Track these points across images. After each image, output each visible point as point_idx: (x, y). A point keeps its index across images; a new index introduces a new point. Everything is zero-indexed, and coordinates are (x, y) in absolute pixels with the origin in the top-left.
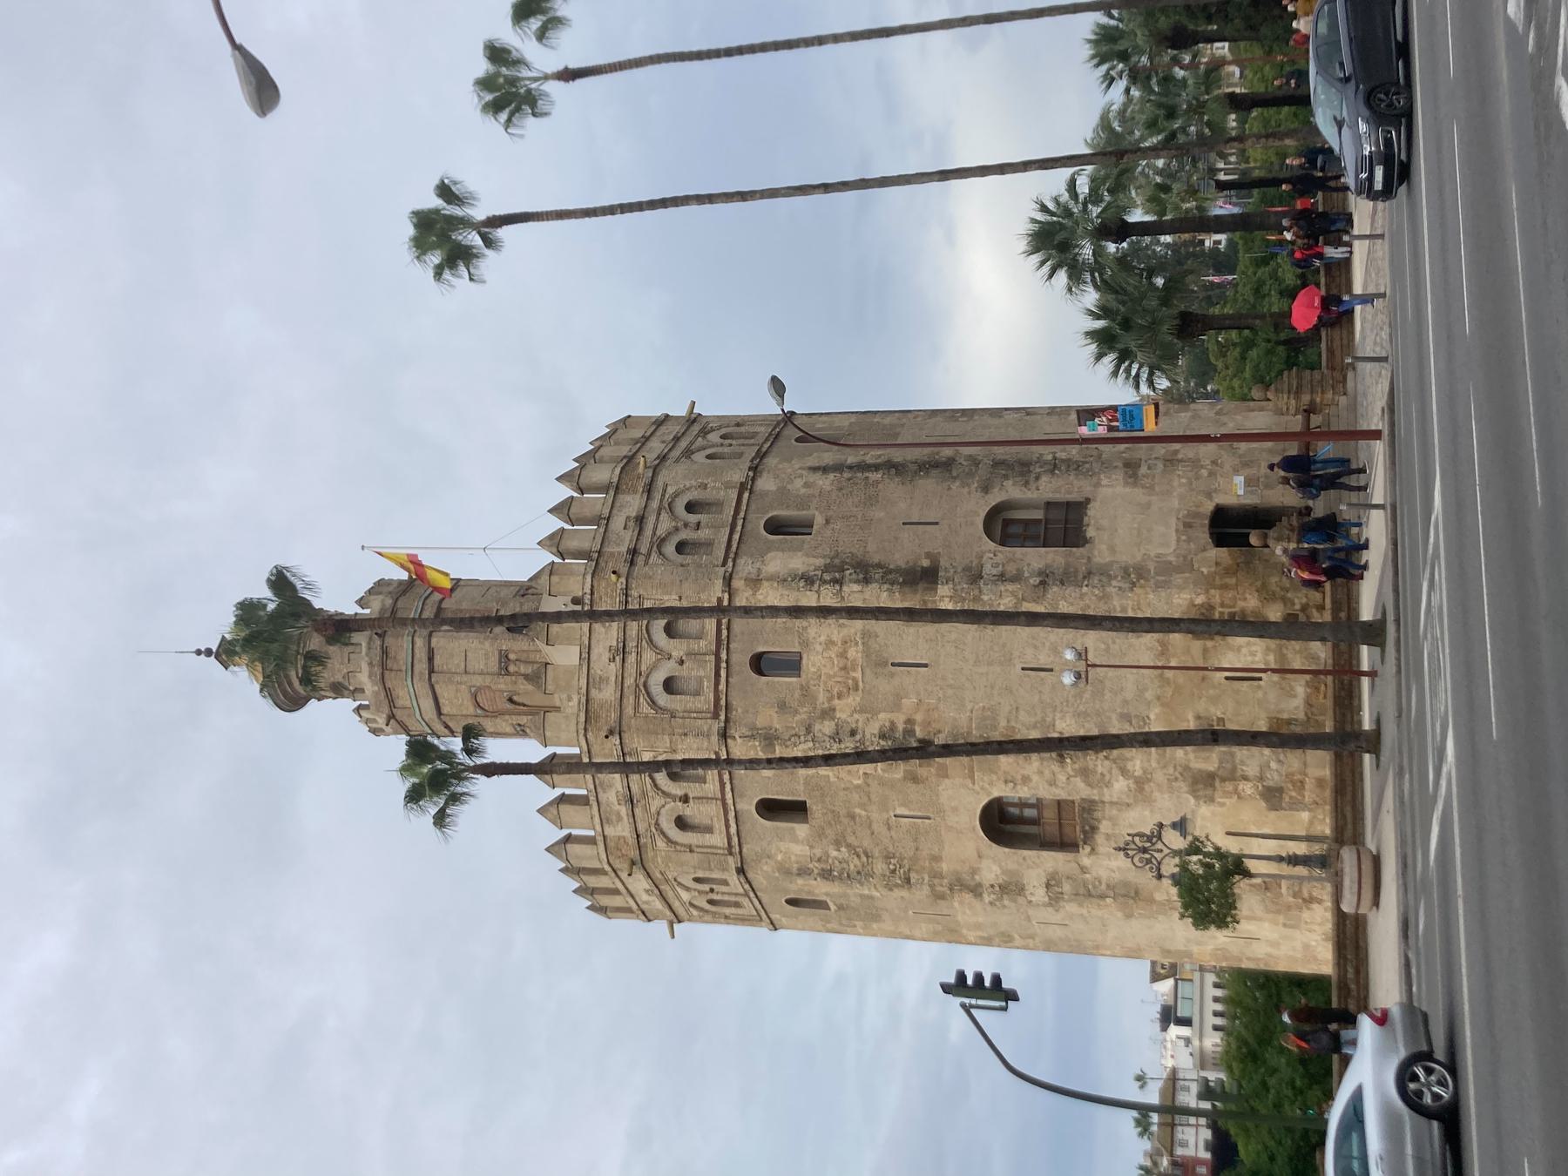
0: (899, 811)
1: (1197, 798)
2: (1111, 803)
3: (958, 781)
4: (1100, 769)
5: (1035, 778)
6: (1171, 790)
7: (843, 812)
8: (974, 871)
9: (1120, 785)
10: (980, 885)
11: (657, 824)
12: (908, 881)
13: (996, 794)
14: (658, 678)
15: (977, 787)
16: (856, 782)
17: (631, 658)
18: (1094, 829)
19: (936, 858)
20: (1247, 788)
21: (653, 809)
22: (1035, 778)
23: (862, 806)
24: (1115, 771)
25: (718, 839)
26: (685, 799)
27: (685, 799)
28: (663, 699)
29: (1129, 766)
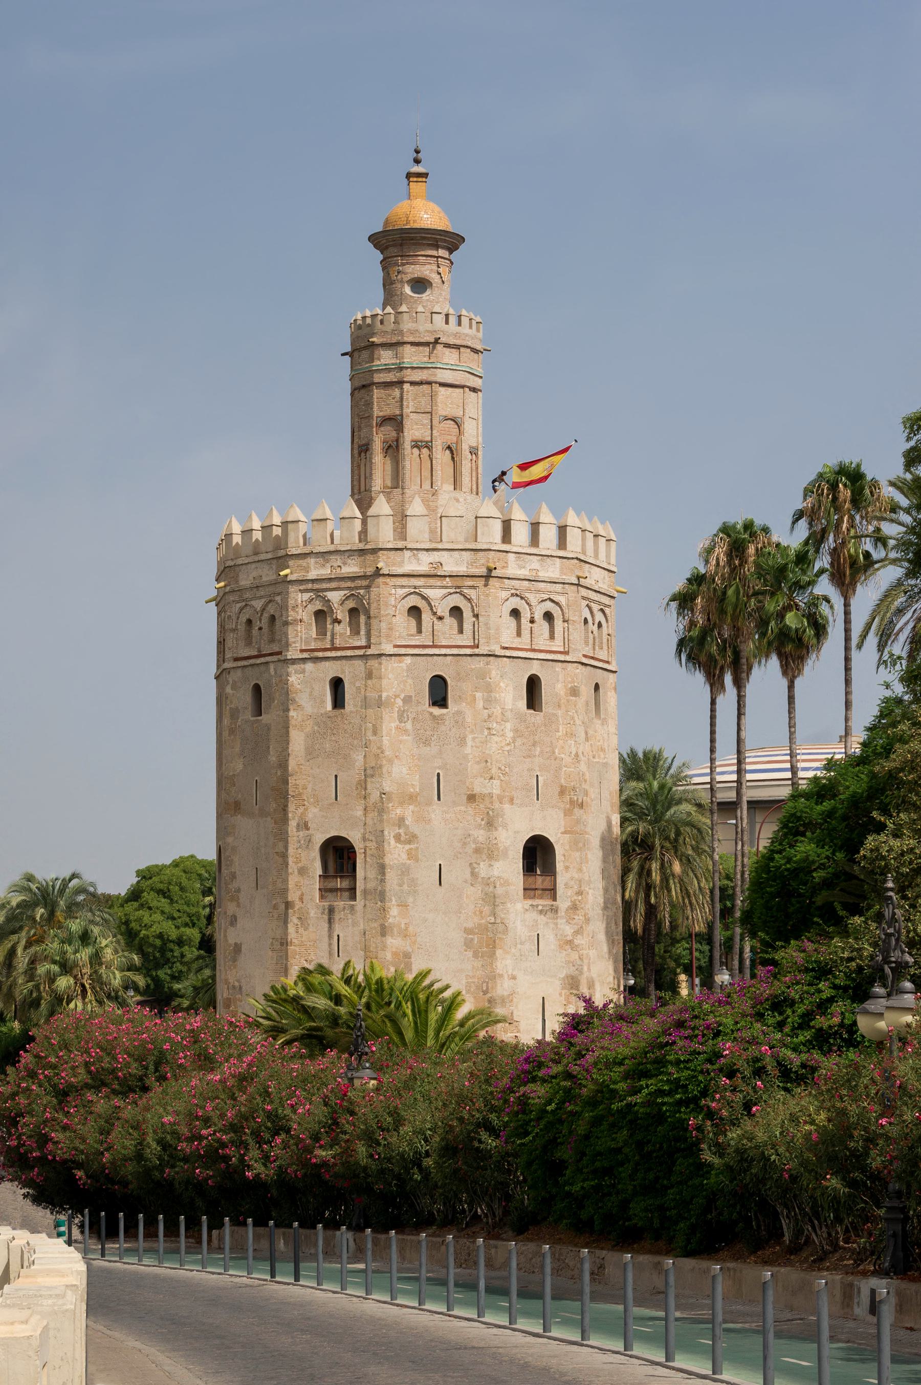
1: (563, 979)
2: (556, 924)
3: (563, 823)
4: (576, 917)
5: (568, 875)
6: (568, 962)
7: (537, 738)
8: (505, 826)
9: (569, 930)
10: (496, 829)
11: (517, 595)
12: (491, 778)
13: (557, 848)
15: (559, 835)
16: (557, 751)
18: (541, 912)
19: (511, 801)
21: (527, 595)
22: (568, 875)
23: (542, 752)
24: (576, 927)
26: (532, 621)
27: (532, 621)
29: (579, 936)
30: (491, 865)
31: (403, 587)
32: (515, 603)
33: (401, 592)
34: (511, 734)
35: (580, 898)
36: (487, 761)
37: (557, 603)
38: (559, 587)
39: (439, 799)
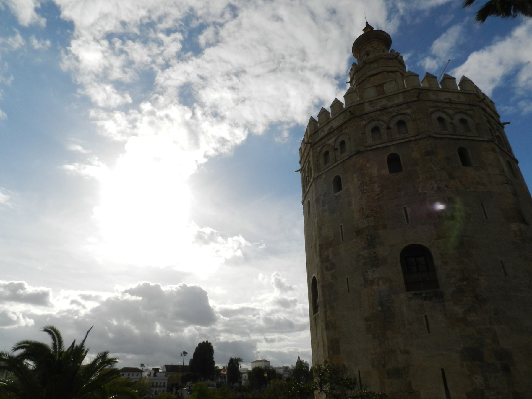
0: (407, 209)
12: (367, 217)
14: (443, 115)
16: (420, 190)
17: (448, 106)
18: (425, 298)
20: (478, 380)
25: (370, 141)
26: (388, 128)
27: (388, 128)
28: (435, 116)
30: (374, 271)
31: (319, 146)
32: (373, 124)
33: (319, 149)
34: (379, 189)
35: (465, 283)
36: (363, 209)
37: (405, 114)
38: (404, 106)
39: (343, 240)
